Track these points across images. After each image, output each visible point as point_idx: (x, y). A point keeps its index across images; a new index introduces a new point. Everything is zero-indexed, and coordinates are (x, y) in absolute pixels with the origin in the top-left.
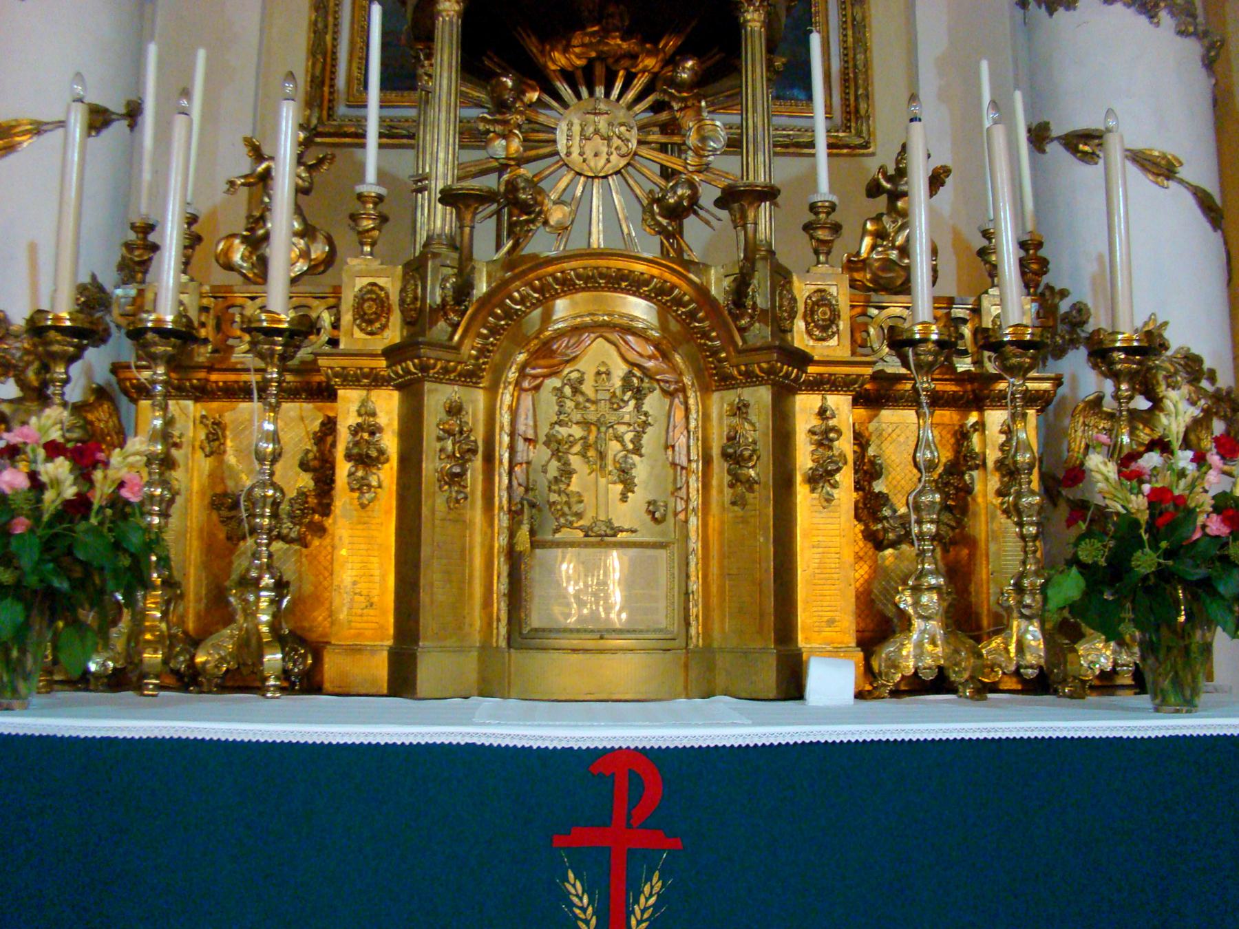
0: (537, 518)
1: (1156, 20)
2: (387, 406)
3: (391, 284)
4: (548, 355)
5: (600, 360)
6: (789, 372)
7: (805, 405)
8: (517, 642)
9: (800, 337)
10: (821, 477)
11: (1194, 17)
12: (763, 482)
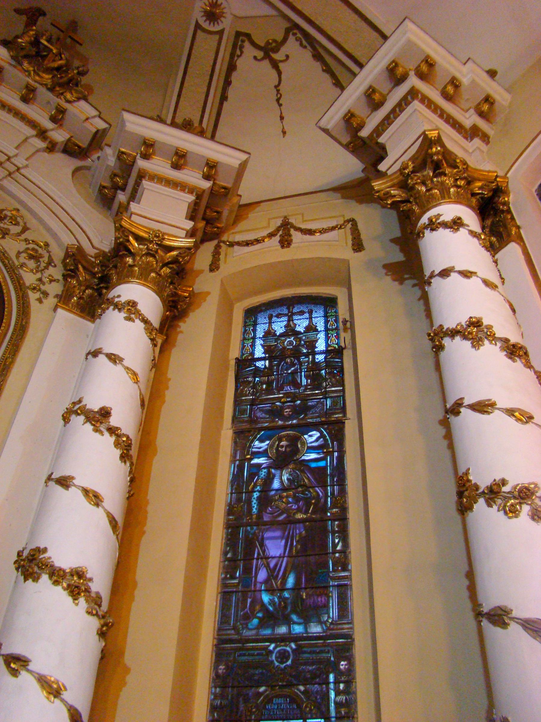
1: (77, 602)
11: (100, 606)
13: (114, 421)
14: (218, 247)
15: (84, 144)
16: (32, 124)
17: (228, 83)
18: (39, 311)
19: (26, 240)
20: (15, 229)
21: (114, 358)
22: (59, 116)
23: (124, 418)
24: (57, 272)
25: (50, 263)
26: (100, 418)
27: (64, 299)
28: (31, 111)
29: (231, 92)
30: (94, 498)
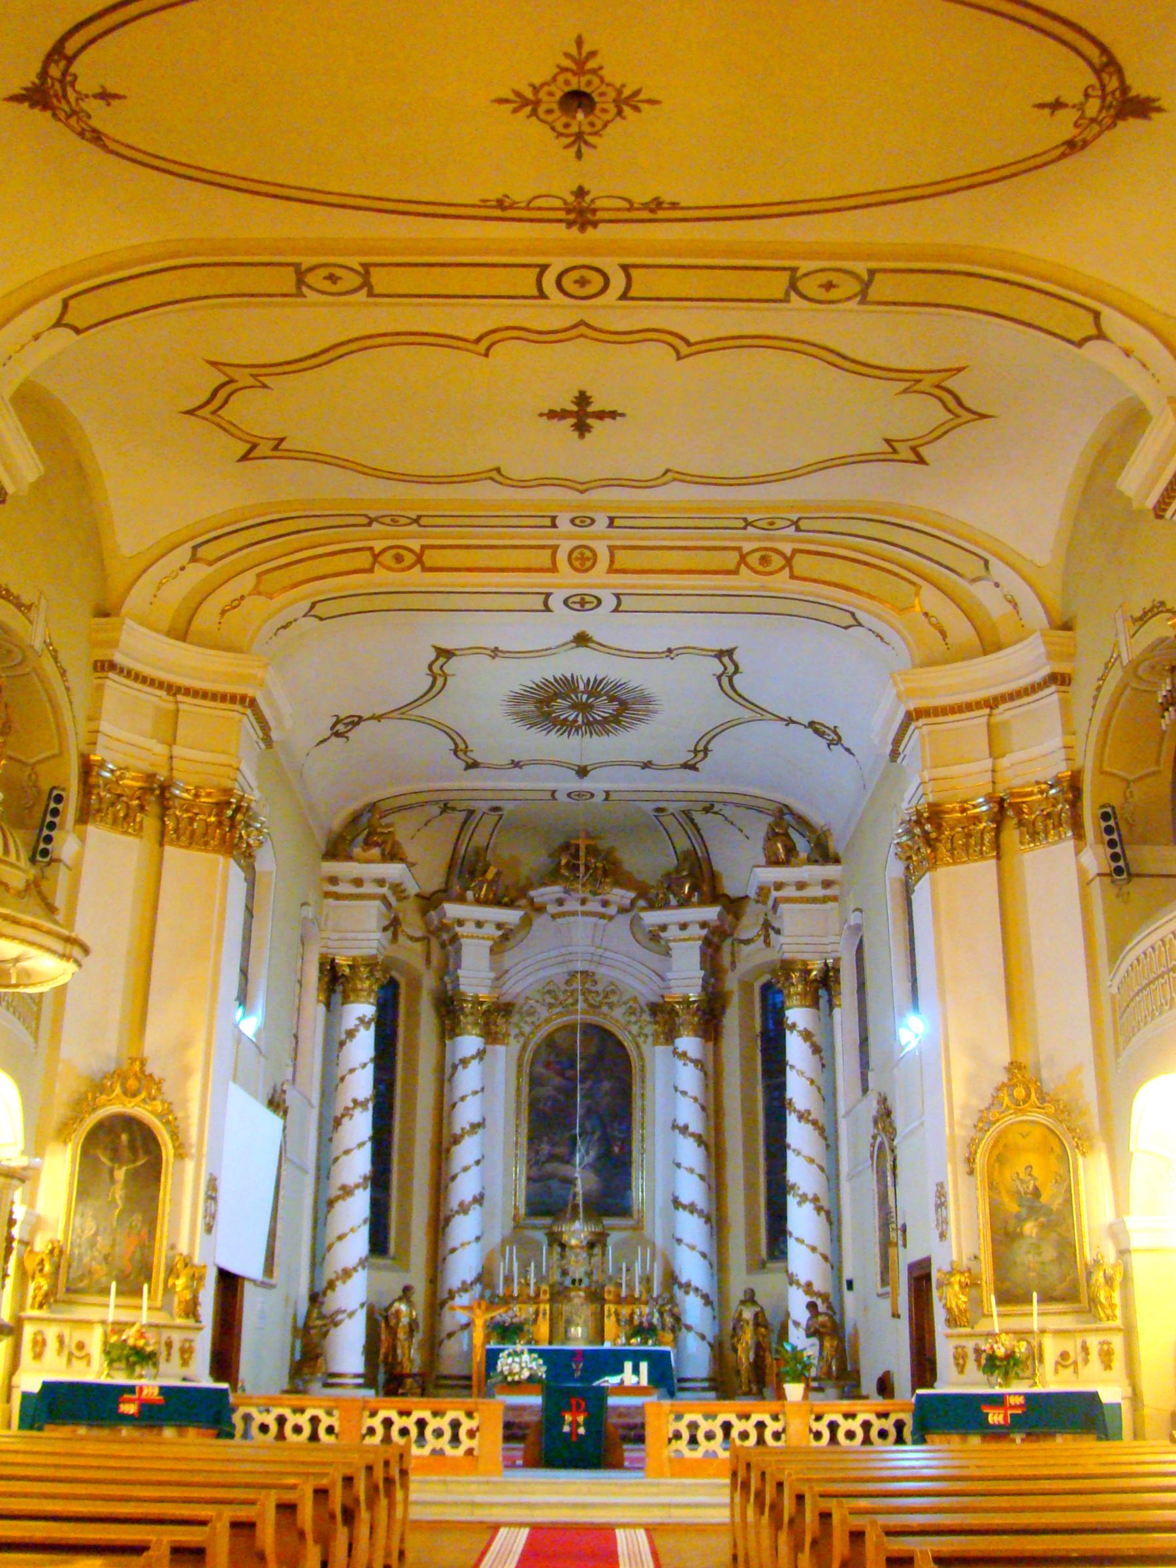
0: (569, 1322)
2: (548, 1307)
3: (547, 1288)
4: (569, 1299)
5: (577, 1301)
6: (603, 1301)
7: (606, 1307)
8: (567, 1338)
9: (606, 1296)
10: (609, 1316)
12: (600, 1318)
14: (733, 944)
15: (628, 906)
16: (594, 914)
17: (695, 825)
18: (645, 1048)
19: (625, 1003)
20: (613, 999)
21: (684, 1093)
22: (605, 904)
23: (696, 1126)
24: (646, 1017)
25: (642, 1011)
26: (684, 1130)
27: (656, 1035)
28: (590, 907)
29: (699, 826)
30: (691, 1171)
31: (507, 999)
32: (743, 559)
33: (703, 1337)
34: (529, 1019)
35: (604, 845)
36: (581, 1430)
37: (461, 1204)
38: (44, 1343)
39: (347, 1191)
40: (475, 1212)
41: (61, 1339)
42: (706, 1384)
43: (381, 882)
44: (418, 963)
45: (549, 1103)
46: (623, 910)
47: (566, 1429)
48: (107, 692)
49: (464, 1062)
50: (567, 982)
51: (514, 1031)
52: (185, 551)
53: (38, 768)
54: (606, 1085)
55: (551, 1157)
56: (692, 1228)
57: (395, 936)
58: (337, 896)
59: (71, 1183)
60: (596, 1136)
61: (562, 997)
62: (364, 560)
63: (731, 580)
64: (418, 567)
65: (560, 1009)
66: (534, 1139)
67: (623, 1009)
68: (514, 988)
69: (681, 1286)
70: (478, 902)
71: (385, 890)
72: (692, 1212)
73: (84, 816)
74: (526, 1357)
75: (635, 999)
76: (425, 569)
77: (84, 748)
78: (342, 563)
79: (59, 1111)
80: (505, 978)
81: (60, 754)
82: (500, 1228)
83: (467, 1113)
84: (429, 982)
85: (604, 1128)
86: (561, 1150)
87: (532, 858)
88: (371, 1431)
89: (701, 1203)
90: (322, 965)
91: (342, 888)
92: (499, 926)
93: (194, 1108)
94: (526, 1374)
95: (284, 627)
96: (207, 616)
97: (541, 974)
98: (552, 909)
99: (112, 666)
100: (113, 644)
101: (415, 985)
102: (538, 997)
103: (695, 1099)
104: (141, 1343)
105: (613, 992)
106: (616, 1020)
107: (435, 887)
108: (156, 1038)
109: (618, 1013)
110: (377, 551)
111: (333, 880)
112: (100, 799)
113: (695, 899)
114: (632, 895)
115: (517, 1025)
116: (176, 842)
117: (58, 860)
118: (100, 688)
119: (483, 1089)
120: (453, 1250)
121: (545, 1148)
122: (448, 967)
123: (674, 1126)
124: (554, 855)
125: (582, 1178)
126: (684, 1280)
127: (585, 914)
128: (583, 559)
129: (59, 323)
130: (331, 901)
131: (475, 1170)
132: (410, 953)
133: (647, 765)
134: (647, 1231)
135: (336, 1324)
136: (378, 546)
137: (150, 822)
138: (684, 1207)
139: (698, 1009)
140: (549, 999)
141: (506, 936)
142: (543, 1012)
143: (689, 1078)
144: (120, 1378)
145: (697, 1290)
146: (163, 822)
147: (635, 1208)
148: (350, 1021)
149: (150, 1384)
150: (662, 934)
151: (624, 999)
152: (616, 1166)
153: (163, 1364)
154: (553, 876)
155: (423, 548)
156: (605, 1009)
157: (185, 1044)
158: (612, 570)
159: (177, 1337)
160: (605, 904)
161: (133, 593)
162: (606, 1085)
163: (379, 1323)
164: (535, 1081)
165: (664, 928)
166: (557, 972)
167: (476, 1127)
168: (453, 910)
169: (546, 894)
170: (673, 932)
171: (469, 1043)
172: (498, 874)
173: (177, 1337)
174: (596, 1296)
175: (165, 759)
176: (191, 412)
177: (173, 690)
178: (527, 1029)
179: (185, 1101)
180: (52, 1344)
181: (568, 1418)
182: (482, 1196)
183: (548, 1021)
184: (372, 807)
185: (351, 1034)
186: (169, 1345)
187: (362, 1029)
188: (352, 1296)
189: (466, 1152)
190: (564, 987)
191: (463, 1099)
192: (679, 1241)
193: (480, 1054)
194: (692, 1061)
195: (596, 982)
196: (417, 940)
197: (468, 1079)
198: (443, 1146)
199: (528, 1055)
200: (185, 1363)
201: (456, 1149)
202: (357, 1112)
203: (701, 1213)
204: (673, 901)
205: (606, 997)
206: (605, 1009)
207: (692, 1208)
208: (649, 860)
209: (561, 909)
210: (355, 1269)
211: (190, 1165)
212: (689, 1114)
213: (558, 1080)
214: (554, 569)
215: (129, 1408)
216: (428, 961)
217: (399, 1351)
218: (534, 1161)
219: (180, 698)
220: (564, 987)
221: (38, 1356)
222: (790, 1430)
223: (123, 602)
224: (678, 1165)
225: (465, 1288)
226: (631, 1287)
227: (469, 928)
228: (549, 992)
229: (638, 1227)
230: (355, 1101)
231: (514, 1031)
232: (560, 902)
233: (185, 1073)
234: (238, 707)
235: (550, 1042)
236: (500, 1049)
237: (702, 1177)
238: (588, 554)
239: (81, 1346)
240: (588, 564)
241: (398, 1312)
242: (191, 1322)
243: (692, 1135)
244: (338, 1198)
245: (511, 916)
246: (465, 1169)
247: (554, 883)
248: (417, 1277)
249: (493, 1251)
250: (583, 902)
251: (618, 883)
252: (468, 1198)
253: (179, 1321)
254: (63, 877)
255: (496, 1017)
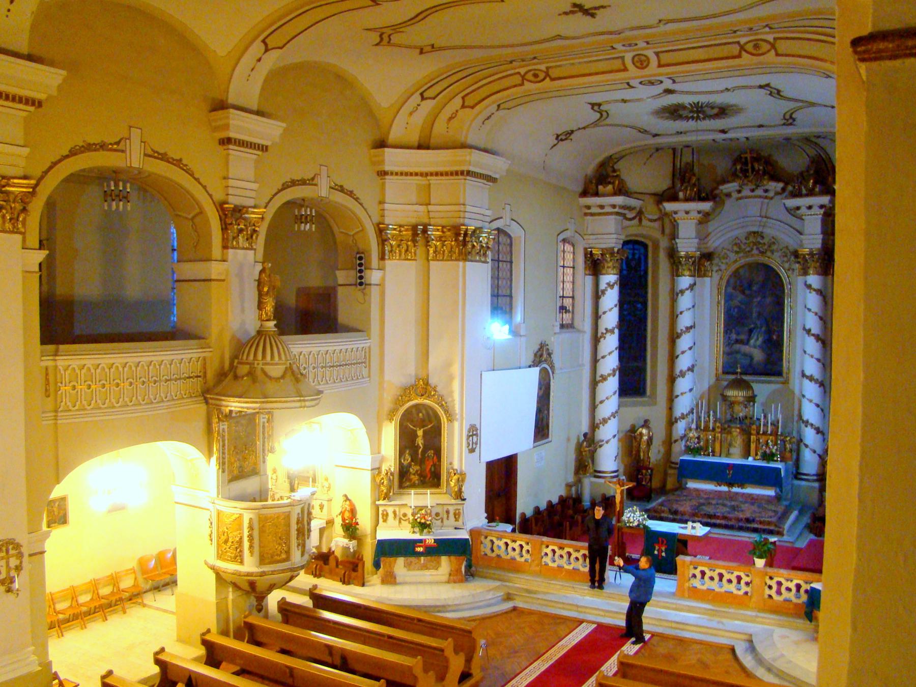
0: (730, 445)
5: (735, 434)
6: (750, 434)
13: (813, 332)
16: (760, 197)
20: (774, 247)
21: (809, 310)
23: (816, 329)
24: (792, 258)
30: (812, 356)
31: (711, 250)
32: (742, 48)
33: (815, 452)
34: (724, 261)
35: (764, 154)
36: (663, 554)
37: (681, 371)
38: (387, 514)
39: (604, 378)
40: (689, 376)
41: (395, 512)
42: (815, 478)
43: (614, 206)
44: (657, 234)
45: (736, 310)
46: (777, 193)
47: (656, 552)
48: (387, 186)
49: (682, 292)
50: (747, 238)
51: (715, 269)
52: (417, 97)
53: (356, 237)
54: (768, 300)
55: (737, 341)
56: (811, 390)
57: (640, 220)
58: (592, 215)
59: (395, 439)
60: (764, 329)
61: (743, 247)
62: (517, 79)
63: (737, 61)
64: (548, 79)
65: (742, 254)
66: (727, 331)
67: (779, 254)
68: (714, 243)
69: (803, 422)
70: (687, 200)
71: (616, 210)
72: (811, 381)
73: (382, 258)
74: (638, 513)
75: (787, 247)
76: (553, 79)
77: (376, 219)
78: (506, 83)
79: (388, 404)
80: (709, 238)
81: (362, 230)
82: (707, 380)
83: (684, 321)
84: (664, 243)
85: (767, 325)
86: (743, 337)
87: (723, 165)
88: (546, 554)
89: (817, 375)
90: (586, 255)
91: (594, 210)
92: (699, 212)
93: (456, 396)
94: (636, 524)
95: (488, 119)
96: (440, 128)
97: (729, 235)
98: (735, 195)
99: (385, 173)
100: (383, 161)
101: (656, 246)
102: (730, 247)
103: (816, 314)
104: (423, 521)
105: (774, 243)
106: (775, 261)
107: (665, 187)
108: (434, 361)
109: (777, 255)
110: (522, 73)
111: (589, 207)
112: (392, 246)
113: (817, 190)
114: (781, 185)
115: (717, 265)
116: (435, 259)
117: (370, 285)
118: (383, 184)
119: (693, 306)
120: (677, 396)
121: (734, 336)
122: (674, 236)
123: (804, 329)
124: (735, 163)
125: (755, 351)
126: (805, 419)
127: (755, 197)
128: (641, 62)
129: (267, 50)
130: (589, 218)
131: (689, 352)
132: (649, 230)
133: (761, 126)
134: (791, 386)
135: (601, 446)
136: (522, 71)
137: (421, 250)
138: (807, 377)
139: (819, 258)
140: (735, 248)
141: (706, 217)
142: (733, 256)
143: (813, 301)
144: (417, 536)
145: (812, 425)
146: (428, 251)
147: (785, 370)
148: (602, 286)
149: (430, 539)
150: (798, 212)
151: (781, 247)
152: (774, 345)
153: (445, 520)
154: (734, 176)
155: (548, 68)
156: (769, 254)
157: (448, 364)
158: (660, 66)
159: (452, 509)
160: (766, 191)
161: (394, 126)
162: (768, 300)
163: (631, 441)
164: (729, 298)
165: (798, 208)
166: (740, 233)
167: (688, 329)
168: (669, 206)
169: (730, 187)
170: (803, 210)
171: (685, 281)
172: (699, 179)
173: (452, 509)
174: (746, 433)
175: (426, 213)
176: (377, 45)
177: (422, 175)
178: (723, 267)
179: (451, 393)
180: (391, 515)
181: (657, 547)
182: (693, 366)
183: (736, 261)
184: (610, 158)
185: (603, 292)
186: (448, 512)
187: (609, 289)
188: (609, 432)
189: (684, 342)
190: (744, 241)
191: (681, 313)
192: (804, 396)
193: (692, 287)
194: (815, 290)
195: (763, 237)
196: (655, 220)
197: (685, 301)
198: (674, 338)
199: (724, 283)
200: (457, 520)
201: (678, 341)
202: (608, 336)
203: (816, 381)
204: (804, 191)
205: (769, 246)
206: (769, 254)
207: (811, 378)
208: (794, 162)
209: (740, 195)
210: (609, 419)
211: (456, 424)
212: (813, 323)
213: (740, 297)
214: (625, 69)
215: (420, 549)
216: (663, 232)
217: (642, 454)
218: (728, 343)
219: (429, 178)
220: (744, 241)
221: (385, 521)
222: (754, 582)
223: (389, 133)
224: (805, 352)
225: (683, 417)
226: (766, 425)
227: (681, 215)
228: (736, 244)
229: (786, 382)
230: (606, 329)
231: (715, 269)
232: (739, 192)
233: (451, 378)
234: (460, 177)
235: (736, 274)
236: (707, 280)
237: (818, 360)
238: (643, 58)
239: (405, 515)
240: (645, 64)
241: (641, 434)
242: (459, 501)
243: (813, 335)
244: (599, 381)
245: (706, 206)
246: (683, 352)
247: (733, 181)
248: (656, 413)
249: (703, 393)
250: (753, 191)
251: (774, 178)
252: (685, 368)
253: (453, 501)
254: (374, 292)
255: (703, 261)
